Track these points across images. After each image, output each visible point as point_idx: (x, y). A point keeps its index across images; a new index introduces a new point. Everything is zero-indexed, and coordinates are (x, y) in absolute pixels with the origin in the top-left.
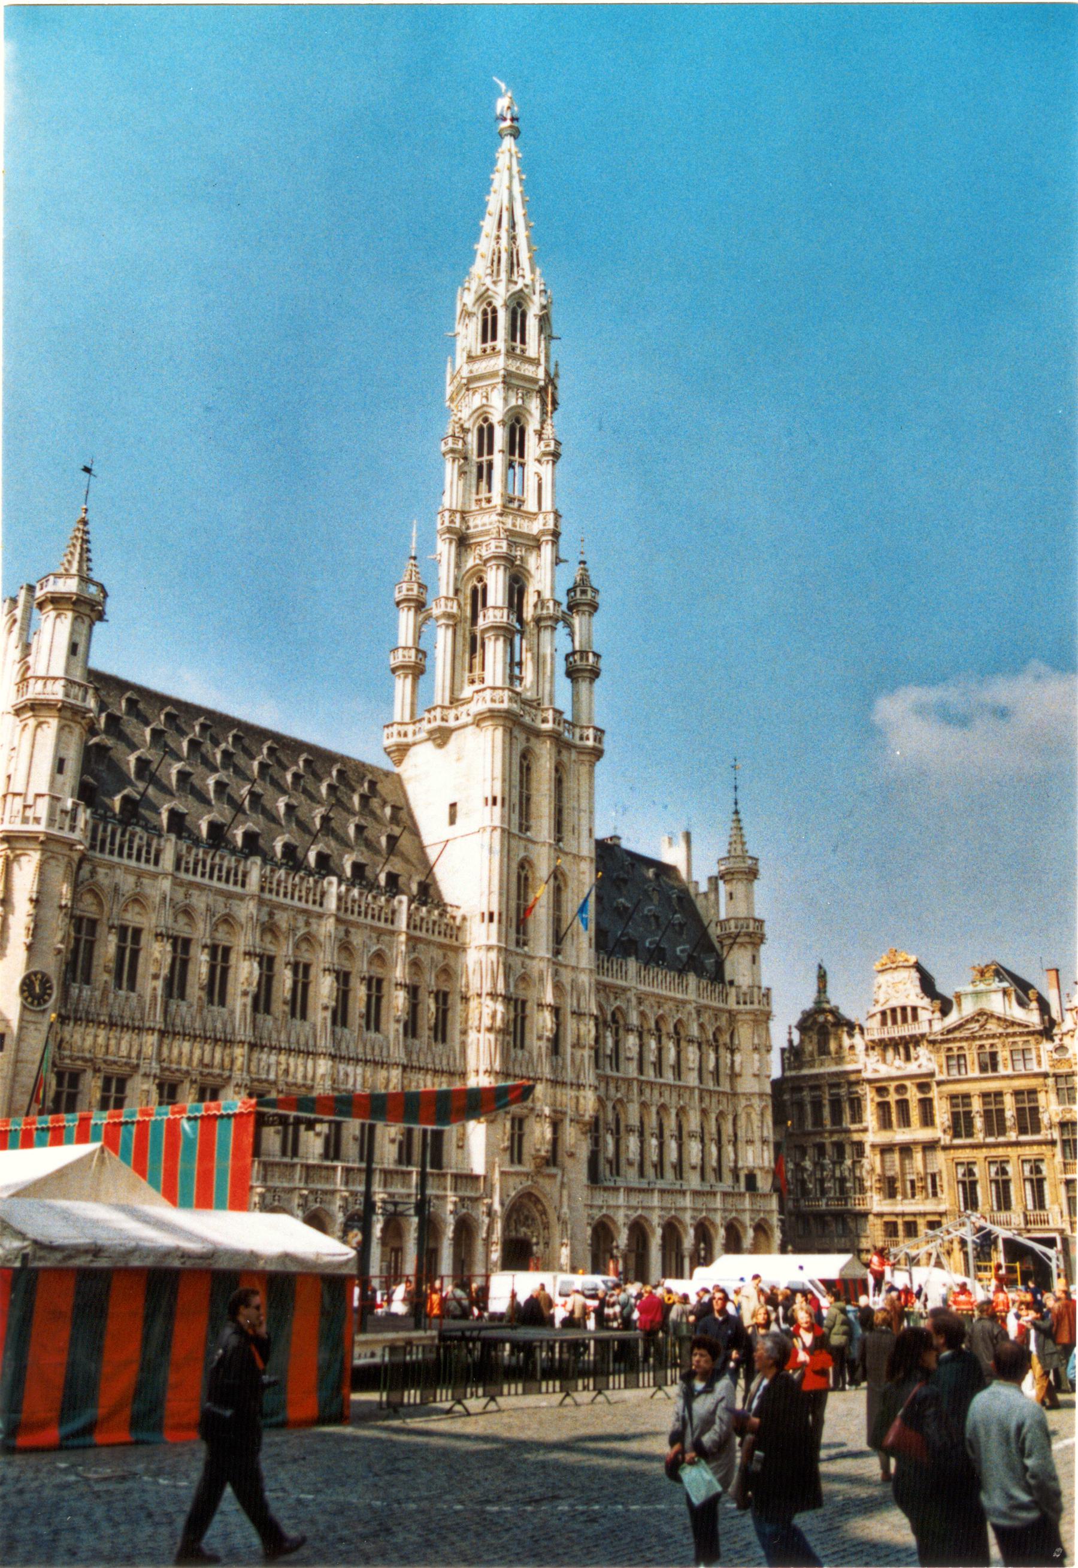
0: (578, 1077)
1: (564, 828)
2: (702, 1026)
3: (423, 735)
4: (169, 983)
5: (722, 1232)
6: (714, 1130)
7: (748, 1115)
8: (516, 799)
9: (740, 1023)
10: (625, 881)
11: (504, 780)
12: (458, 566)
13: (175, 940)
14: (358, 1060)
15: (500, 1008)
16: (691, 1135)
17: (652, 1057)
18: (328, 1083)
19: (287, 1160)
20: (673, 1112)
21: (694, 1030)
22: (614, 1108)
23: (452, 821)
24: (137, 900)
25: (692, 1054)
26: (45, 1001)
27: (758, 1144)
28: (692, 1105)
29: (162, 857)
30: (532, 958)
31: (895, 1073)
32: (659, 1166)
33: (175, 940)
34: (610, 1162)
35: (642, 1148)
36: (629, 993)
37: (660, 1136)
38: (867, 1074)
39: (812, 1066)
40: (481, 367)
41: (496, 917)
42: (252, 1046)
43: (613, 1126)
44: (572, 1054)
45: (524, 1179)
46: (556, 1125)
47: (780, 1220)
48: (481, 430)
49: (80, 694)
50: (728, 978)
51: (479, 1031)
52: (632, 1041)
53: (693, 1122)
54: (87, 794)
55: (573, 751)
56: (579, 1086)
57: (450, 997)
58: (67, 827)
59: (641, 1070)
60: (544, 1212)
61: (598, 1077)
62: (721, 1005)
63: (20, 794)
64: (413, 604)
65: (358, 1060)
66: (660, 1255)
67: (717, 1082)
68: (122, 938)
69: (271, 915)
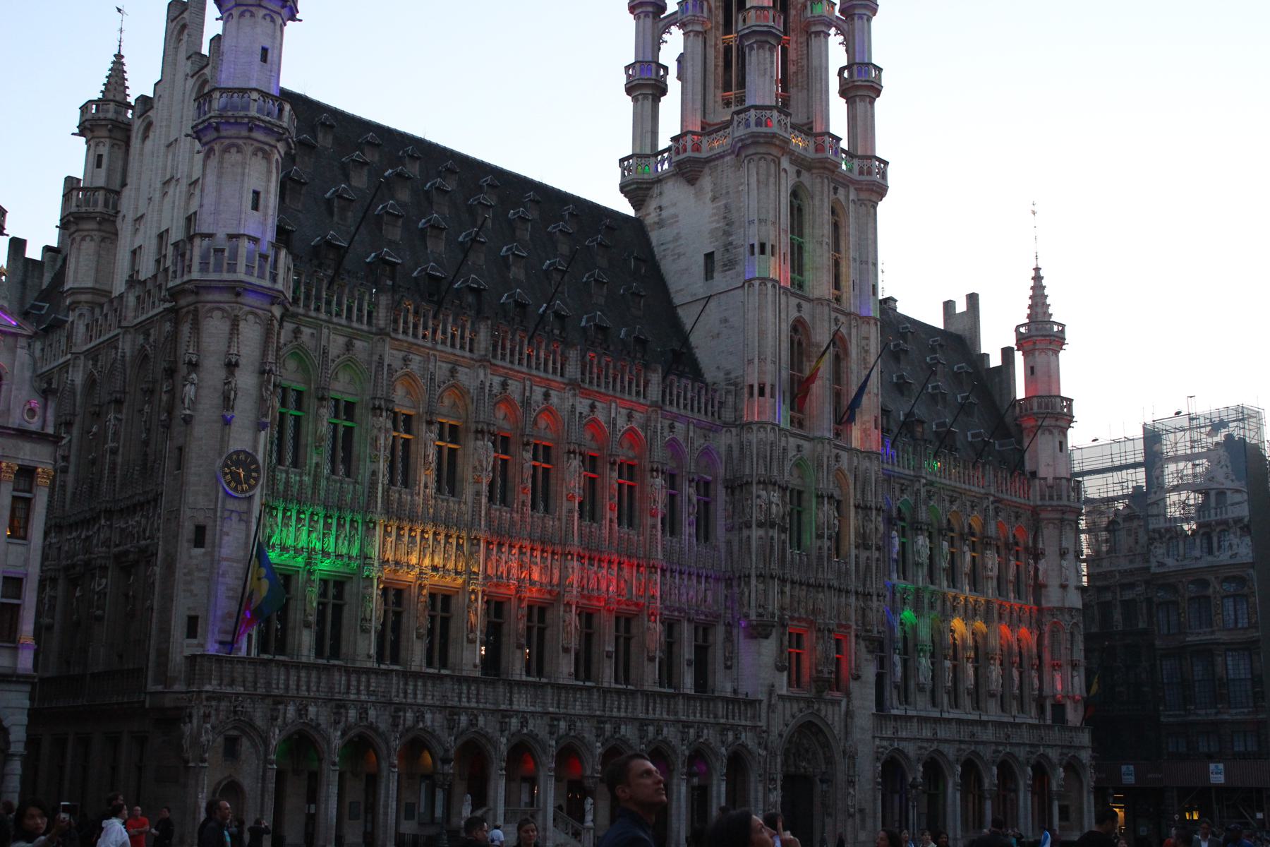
0: (864, 585)
1: (843, 284)
2: (999, 525)
5: (1029, 769)
8: (785, 247)
10: (906, 352)
11: (774, 223)
15: (775, 496)
25: (992, 560)
26: (252, 487)
29: (375, 314)
32: (954, 694)
34: (897, 687)
36: (917, 486)
41: (768, 390)
43: (900, 645)
44: (857, 557)
45: (802, 705)
46: (838, 642)
47: (1093, 758)
51: (749, 527)
52: (922, 541)
54: (283, 236)
56: (867, 596)
57: (712, 486)
59: (932, 577)
62: (1022, 501)
63: (210, 236)
64: (650, 9)
66: (958, 795)
69: (504, 385)
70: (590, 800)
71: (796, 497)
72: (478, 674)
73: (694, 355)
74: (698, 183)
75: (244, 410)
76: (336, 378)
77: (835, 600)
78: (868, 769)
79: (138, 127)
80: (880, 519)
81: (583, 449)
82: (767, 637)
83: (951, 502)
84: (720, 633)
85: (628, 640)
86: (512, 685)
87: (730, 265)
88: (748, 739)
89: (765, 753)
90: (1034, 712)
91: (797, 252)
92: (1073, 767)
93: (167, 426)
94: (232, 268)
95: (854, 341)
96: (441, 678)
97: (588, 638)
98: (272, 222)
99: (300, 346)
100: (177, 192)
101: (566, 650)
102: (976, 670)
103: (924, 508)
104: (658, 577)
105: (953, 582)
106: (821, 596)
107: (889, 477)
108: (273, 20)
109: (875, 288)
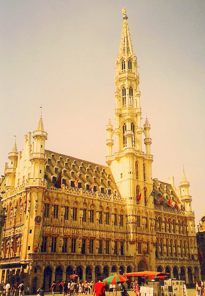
1: (146, 178)
3: (114, 159)
4: (65, 216)
6: (183, 245)
9: (187, 220)
11: (132, 168)
12: (120, 121)
14: (105, 231)
16: (178, 246)
18: (99, 236)
19: (91, 254)
20: (174, 241)
21: (177, 222)
22: (160, 240)
24: (57, 199)
27: (194, 248)
28: (178, 239)
32: (171, 254)
37: (171, 246)
40: (122, 76)
41: (132, 198)
42: (82, 229)
46: (148, 244)
48: (123, 90)
49: (44, 156)
52: (163, 224)
53: (179, 243)
54: (46, 177)
55: (147, 161)
56: (153, 235)
58: (42, 185)
60: (146, 265)
61: (156, 233)
64: (110, 130)
65: (105, 231)
68: (55, 208)
69: (85, 200)
71: (138, 217)
72: (81, 254)
74: (119, 161)
76: (55, 201)
77: (146, 236)
80: (154, 221)
81: (99, 211)
82: (134, 244)
85: (108, 246)
86: (87, 256)
88: (132, 265)
89: (134, 267)
90: (188, 257)
91: (137, 172)
92: (196, 268)
93: (25, 212)
95: (148, 188)
97: (101, 246)
98: (43, 175)
99: (49, 196)
103: (163, 218)
105: (170, 231)
106: (144, 236)
107: (156, 213)
108: (43, 140)
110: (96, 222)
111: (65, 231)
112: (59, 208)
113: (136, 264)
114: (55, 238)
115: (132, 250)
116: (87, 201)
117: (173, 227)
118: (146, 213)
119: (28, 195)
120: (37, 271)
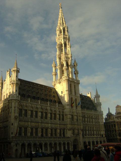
2: (95, 116)
3: (57, 83)
4: (31, 116)
5: (99, 142)
7: (101, 127)
12: (60, 62)
13: (31, 111)
15: (70, 116)
16: (94, 130)
17: (89, 121)
18: (50, 127)
19: (46, 136)
20: (92, 128)
23: (62, 93)
24: (26, 106)
30: (73, 110)
31: (119, 121)
33: (31, 111)
35: (89, 132)
37: (91, 131)
38: (116, 121)
39: (108, 121)
42: (41, 123)
46: (78, 130)
48: (61, 44)
50: (97, 110)
52: (86, 119)
53: (95, 129)
54: (19, 94)
56: (81, 125)
67: (97, 124)
69: (42, 107)
70: (53, 149)
71: (72, 116)
72: (40, 136)
73: (61, 102)
75: (16, 111)
78: (82, 143)
79: (4, 83)
83: (89, 114)
84: (65, 130)
87: (64, 92)
90: (100, 136)
93: (9, 113)
94: (14, 98)
96: (37, 137)
97: (52, 132)
98: (18, 93)
100: (8, 90)
101: (50, 133)
102: (93, 132)
104: (58, 125)
105: (90, 123)
107: (82, 113)
109: (79, 93)
110: (49, 119)
111: (31, 124)
112: (27, 111)
113: (72, 141)
114: (26, 129)
115: (69, 134)
116: (43, 107)
117: (91, 120)
118: (77, 113)
119: (10, 104)
120: (17, 146)
